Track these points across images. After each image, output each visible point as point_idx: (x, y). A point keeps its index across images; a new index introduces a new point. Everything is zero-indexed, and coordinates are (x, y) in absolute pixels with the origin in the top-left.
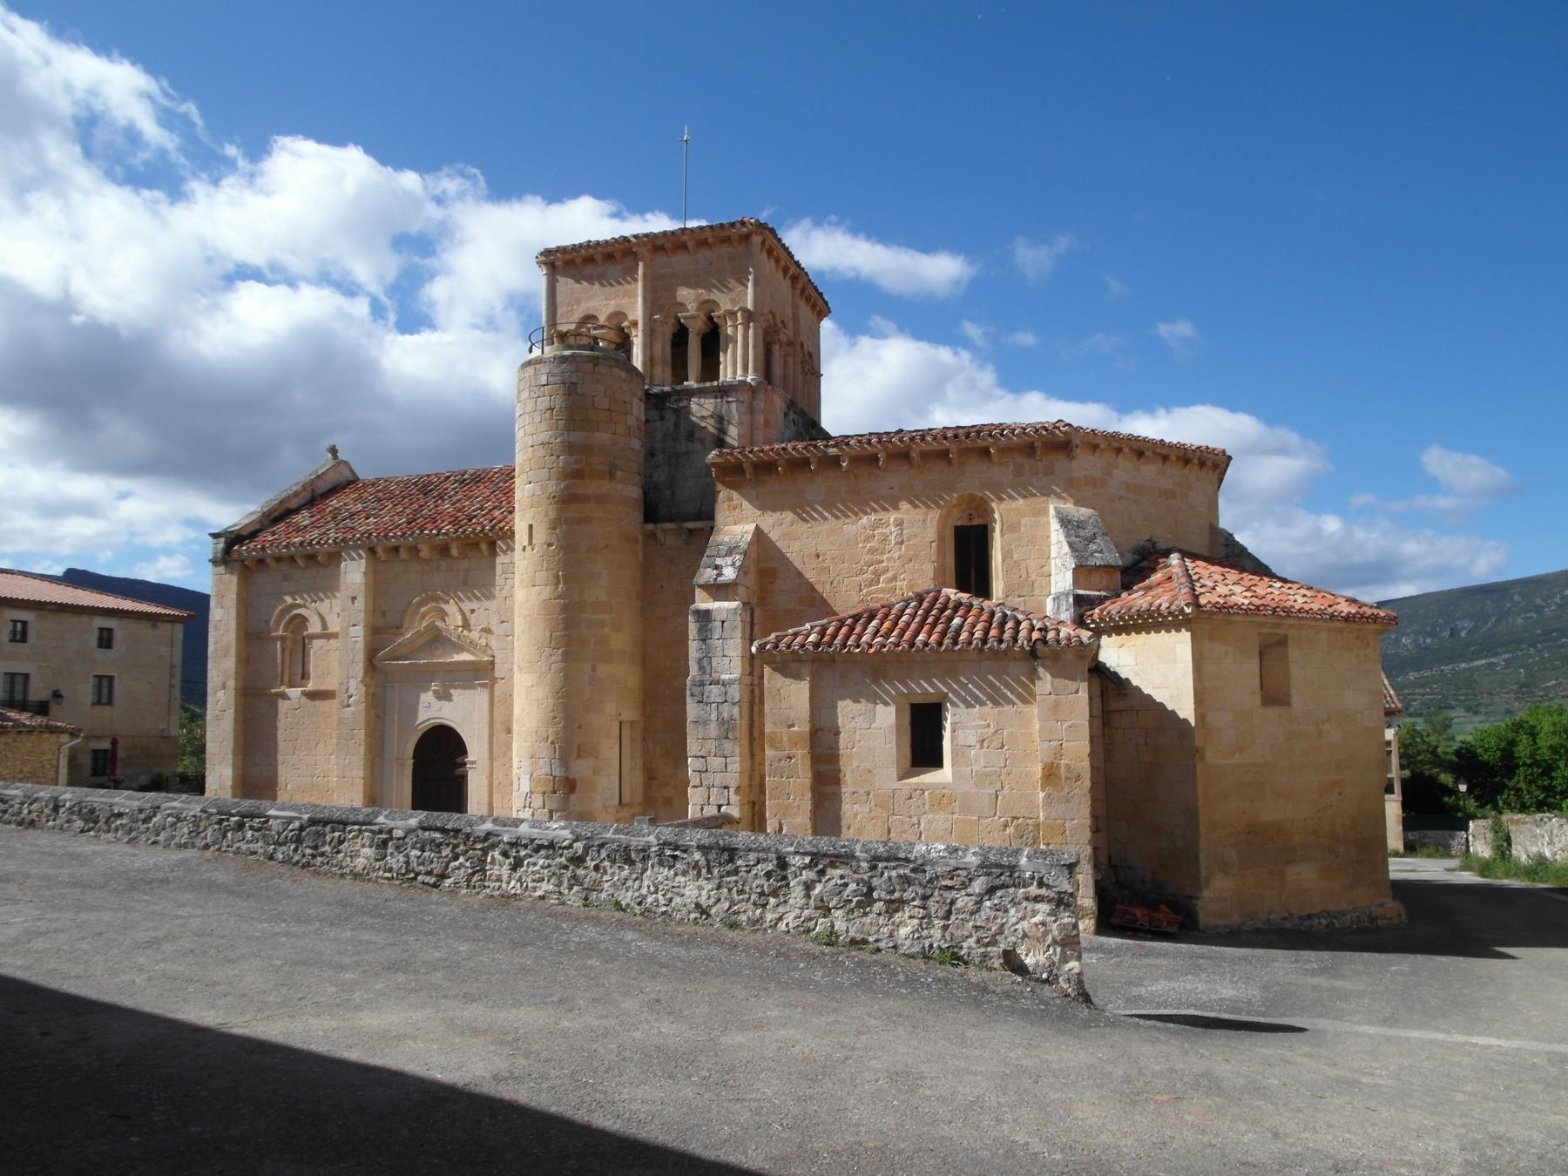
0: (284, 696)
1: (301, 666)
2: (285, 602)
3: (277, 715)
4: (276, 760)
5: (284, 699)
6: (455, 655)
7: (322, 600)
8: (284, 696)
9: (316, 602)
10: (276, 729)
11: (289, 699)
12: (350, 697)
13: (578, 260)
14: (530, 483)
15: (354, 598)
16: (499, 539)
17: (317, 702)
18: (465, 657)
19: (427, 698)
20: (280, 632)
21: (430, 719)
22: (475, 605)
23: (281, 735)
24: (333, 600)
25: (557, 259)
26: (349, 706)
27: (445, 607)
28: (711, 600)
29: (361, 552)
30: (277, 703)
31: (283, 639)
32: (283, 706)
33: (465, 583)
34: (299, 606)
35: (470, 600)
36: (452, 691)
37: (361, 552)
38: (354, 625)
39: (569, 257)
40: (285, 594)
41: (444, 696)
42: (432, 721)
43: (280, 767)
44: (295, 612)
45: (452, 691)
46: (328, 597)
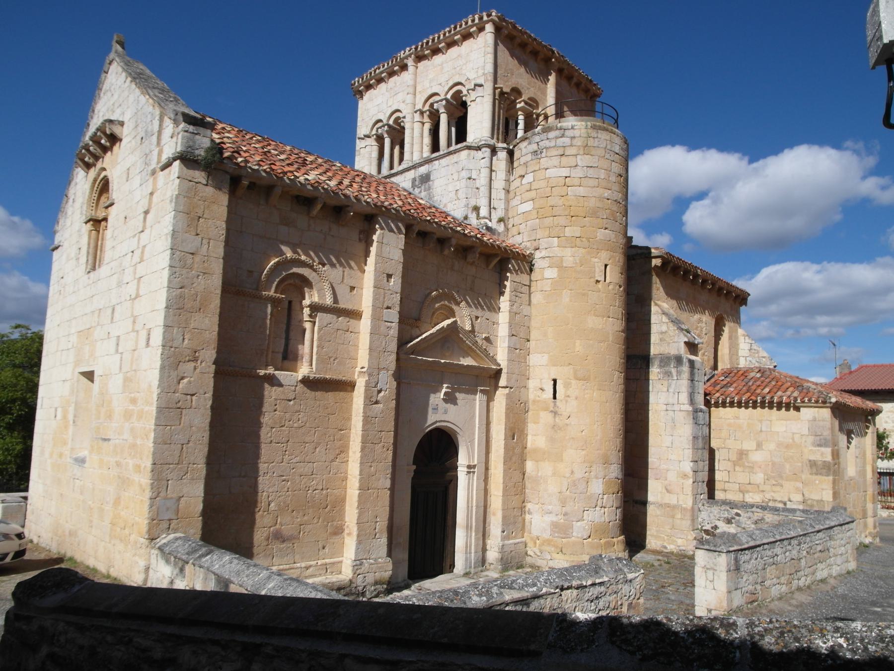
0: (272, 381)
1: (283, 341)
2: (282, 253)
3: (261, 404)
4: (256, 470)
5: (272, 385)
6: (461, 359)
7: (333, 265)
8: (272, 381)
9: (324, 265)
10: (259, 425)
11: (280, 385)
12: (380, 391)
13: (518, 41)
14: (606, 229)
15: (389, 276)
16: (513, 258)
17: (319, 394)
18: (467, 361)
19: (437, 399)
20: (272, 293)
21: (448, 422)
22: (479, 313)
23: (265, 434)
24: (347, 270)
25: (507, 28)
26: (377, 402)
27: (454, 307)
28: (689, 353)
29: (400, 225)
30: (263, 389)
31: (275, 302)
32: (271, 393)
33: (472, 289)
34: (303, 264)
35: (477, 308)
36: (457, 395)
37: (400, 225)
38: (388, 308)
39: (515, 33)
40: (283, 243)
41: (450, 399)
42: (438, 424)
43: (260, 479)
44: (295, 270)
45: (457, 395)
46: (341, 265)
